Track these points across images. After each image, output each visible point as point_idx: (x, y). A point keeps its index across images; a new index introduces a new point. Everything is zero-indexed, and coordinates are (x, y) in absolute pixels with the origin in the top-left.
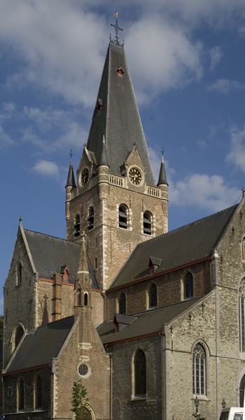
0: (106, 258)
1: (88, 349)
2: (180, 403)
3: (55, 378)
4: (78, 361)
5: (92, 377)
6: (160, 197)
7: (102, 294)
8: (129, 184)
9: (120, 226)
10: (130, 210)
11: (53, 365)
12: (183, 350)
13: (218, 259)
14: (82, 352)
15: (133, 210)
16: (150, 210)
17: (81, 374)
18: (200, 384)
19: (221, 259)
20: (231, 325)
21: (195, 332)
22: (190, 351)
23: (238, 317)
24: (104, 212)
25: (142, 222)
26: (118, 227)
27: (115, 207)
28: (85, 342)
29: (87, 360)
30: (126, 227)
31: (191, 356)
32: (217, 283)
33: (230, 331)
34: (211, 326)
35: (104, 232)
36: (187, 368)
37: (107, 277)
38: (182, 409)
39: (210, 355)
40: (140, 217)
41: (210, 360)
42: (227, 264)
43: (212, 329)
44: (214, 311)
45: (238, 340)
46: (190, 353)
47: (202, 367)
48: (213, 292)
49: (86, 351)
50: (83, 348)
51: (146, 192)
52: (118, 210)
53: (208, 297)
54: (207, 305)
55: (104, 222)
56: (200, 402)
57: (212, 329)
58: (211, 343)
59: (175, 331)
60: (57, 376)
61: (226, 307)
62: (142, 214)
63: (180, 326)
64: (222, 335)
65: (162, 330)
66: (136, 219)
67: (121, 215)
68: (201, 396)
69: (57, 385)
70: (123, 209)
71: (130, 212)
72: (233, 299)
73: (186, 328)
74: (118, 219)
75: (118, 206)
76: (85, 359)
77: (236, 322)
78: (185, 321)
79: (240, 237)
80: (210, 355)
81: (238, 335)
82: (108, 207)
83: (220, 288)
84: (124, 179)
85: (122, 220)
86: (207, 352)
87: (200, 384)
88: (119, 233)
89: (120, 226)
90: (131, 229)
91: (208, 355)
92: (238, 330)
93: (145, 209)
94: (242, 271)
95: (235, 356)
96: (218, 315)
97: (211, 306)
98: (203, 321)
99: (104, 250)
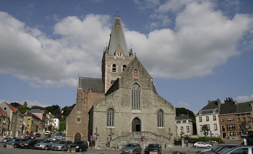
0: (107, 82)
1: (80, 113)
2: (100, 130)
3: (67, 123)
4: (76, 117)
5: (81, 123)
6: (130, 59)
7: (105, 95)
8: (117, 58)
9: (113, 71)
10: (117, 66)
11: (67, 119)
12: (102, 111)
13: (120, 78)
14: (78, 114)
15: (118, 65)
16: (125, 64)
17: (77, 121)
18: (110, 122)
19: (122, 78)
20: (127, 101)
21: (108, 105)
22: (105, 111)
23: (131, 98)
24: (106, 68)
25: (122, 69)
26: (112, 72)
27: (111, 66)
28: (78, 111)
29: (79, 117)
30: (115, 72)
31: (106, 113)
32: (120, 87)
33: (127, 103)
34: (117, 102)
35: (106, 74)
36: (104, 117)
37: (107, 89)
38: (101, 132)
39: (116, 112)
40: (121, 67)
41: (116, 114)
42: (125, 79)
43: (117, 103)
44: (118, 96)
45: (131, 106)
46: (105, 112)
47: (113, 117)
48: (118, 90)
49: (79, 114)
50: (78, 113)
51: (124, 59)
52: (112, 67)
53: (115, 92)
54: (115, 95)
55: (106, 71)
56: (112, 129)
57: (117, 103)
58: (116, 109)
59: (98, 105)
60: (68, 123)
61: (125, 95)
62: (122, 67)
63: (101, 103)
64: (122, 105)
65: (11, 104)
66: (119, 68)
67: (113, 68)
68: (113, 127)
69: (68, 126)
70: (114, 65)
71: (117, 66)
72: (128, 91)
73: (104, 104)
74: (112, 70)
75: (112, 65)
76: (79, 117)
77: (130, 99)
78: (104, 101)
79: (132, 70)
80: (116, 112)
81: (131, 104)
82: (108, 66)
83: (122, 88)
84: (114, 57)
85: (114, 69)
86: (115, 111)
87: (110, 122)
88: (112, 73)
89: (113, 71)
90: (117, 72)
91: (115, 112)
92: (131, 102)
93: (123, 64)
94: (133, 81)
95: (129, 112)
96: (120, 98)
97: (117, 95)
98: (113, 100)
99: (106, 80)
